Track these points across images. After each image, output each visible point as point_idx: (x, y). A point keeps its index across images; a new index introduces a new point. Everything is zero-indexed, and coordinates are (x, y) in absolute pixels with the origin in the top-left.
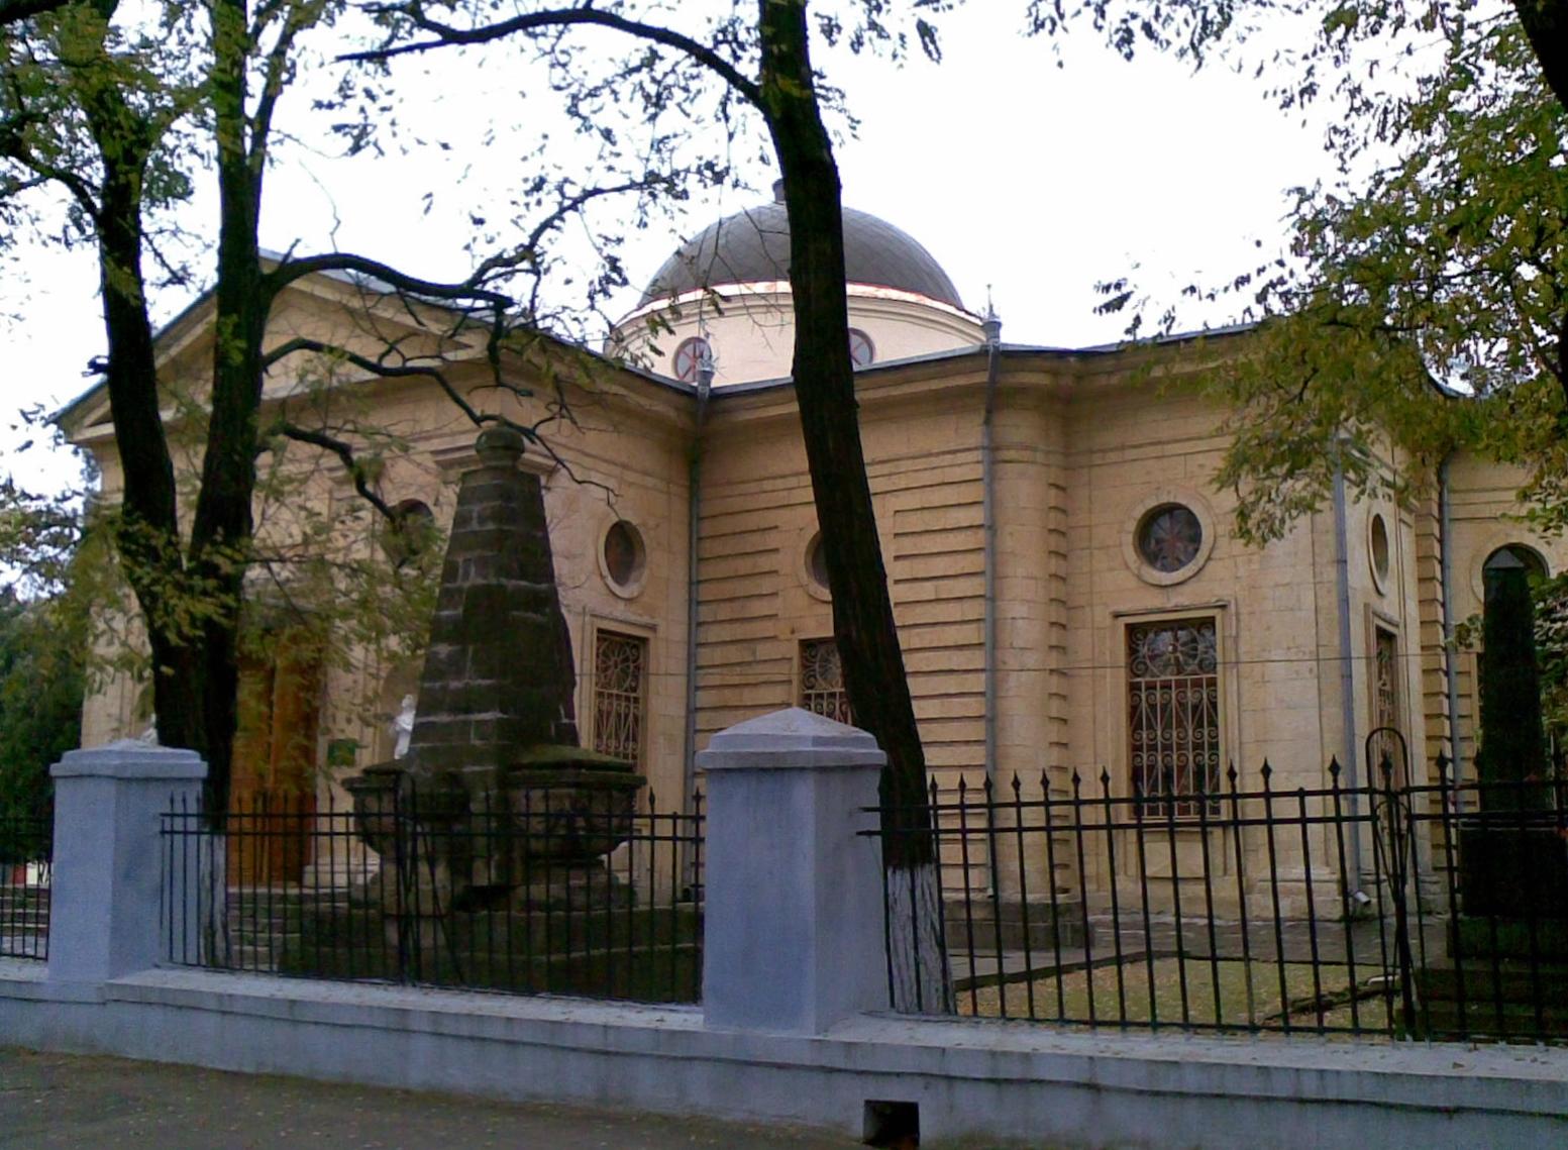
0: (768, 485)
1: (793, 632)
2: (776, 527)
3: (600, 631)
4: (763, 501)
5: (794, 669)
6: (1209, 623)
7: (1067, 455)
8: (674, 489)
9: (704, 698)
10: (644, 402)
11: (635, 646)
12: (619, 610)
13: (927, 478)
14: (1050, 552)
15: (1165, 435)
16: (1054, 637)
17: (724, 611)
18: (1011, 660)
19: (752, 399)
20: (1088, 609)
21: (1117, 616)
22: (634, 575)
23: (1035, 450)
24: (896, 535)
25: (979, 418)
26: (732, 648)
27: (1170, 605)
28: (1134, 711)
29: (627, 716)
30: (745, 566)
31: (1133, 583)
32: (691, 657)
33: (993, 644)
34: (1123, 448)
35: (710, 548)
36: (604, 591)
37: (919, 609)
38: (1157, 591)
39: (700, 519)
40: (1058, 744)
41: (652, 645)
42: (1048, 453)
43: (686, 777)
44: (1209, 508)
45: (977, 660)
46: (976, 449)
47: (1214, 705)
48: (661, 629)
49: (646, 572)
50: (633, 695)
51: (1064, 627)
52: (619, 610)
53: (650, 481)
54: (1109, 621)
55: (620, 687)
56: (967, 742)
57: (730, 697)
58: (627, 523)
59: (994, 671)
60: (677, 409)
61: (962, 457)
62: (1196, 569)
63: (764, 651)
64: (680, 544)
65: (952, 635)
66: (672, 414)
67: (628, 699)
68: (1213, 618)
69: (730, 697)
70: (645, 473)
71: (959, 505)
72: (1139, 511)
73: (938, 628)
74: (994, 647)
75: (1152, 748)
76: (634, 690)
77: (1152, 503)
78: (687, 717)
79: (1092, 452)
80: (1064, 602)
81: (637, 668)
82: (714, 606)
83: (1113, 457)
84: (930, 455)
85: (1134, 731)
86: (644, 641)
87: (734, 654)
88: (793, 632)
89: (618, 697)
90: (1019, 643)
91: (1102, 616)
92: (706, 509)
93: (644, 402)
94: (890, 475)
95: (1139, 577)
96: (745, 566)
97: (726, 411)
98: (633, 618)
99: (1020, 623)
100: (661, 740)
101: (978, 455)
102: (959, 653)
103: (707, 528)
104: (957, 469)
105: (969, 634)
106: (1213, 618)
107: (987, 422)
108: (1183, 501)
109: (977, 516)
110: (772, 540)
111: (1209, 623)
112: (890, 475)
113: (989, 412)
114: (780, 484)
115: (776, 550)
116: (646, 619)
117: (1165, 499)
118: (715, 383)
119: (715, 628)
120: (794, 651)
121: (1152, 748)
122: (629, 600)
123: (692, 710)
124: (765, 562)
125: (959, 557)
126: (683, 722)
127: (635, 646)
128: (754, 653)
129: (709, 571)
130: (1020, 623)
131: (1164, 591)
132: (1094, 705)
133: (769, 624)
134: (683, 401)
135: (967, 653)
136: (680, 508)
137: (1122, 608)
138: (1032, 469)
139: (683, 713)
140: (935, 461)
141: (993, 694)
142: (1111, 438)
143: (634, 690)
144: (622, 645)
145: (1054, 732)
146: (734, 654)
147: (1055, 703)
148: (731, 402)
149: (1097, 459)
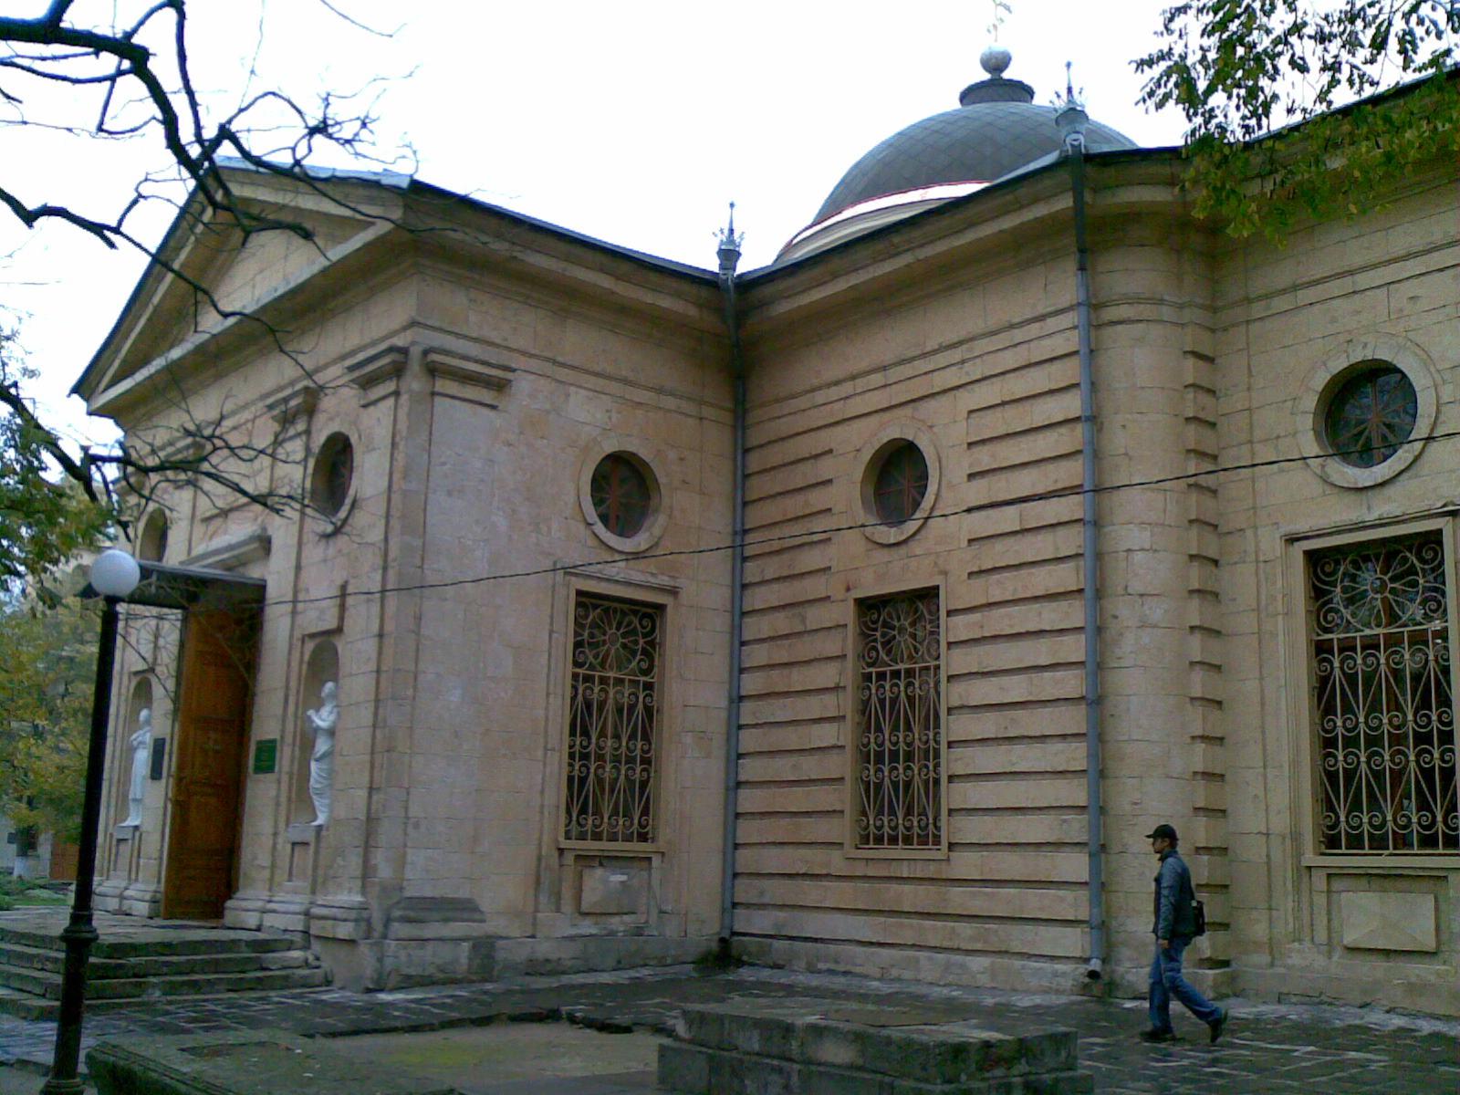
0: (820, 397)
1: (848, 589)
2: (831, 451)
3: (579, 593)
4: (817, 418)
5: (847, 642)
6: (1434, 538)
7: (1215, 310)
8: (707, 412)
9: (751, 684)
10: (649, 298)
11: (645, 615)
12: (619, 570)
13: (1010, 359)
14: (1189, 451)
15: (1358, 261)
16: (1196, 576)
17: (772, 568)
18: (1124, 612)
19: (790, 282)
20: (1249, 533)
21: (1292, 540)
22: (647, 524)
23: (1161, 302)
24: (970, 445)
25: (1071, 265)
26: (781, 615)
27: (1371, 517)
28: (1322, 687)
29: (632, 708)
30: (794, 505)
31: (1318, 487)
32: (736, 629)
33: (1097, 592)
34: (1295, 288)
35: (757, 487)
36: (591, 541)
37: (999, 546)
38: (1353, 497)
39: (746, 451)
40: (1203, 738)
41: (669, 610)
42: (1181, 307)
43: (727, 789)
44: (1428, 361)
45: (1074, 613)
46: (1070, 308)
47: (1446, 671)
48: (683, 596)
49: (661, 519)
50: (642, 679)
51: (1216, 562)
52: (619, 570)
53: (670, 402)
54: (1279, 546)
55: (619, 669)
56: (1064, 737)
57: (778, 680)
58: (634, 454)
59: (1098, 631)
60: (700, 306)
61: (1052, 324)
62: (1410, 458)
63: (816, 616)
64: (720, 482)
65: (1043, 580)
66: (692, 311)
67: (635, 683)
68: (1439, 532)
69: (778, 680)
70: (660, 391)
71: (1052, 392)
72: (1321, 380)
73: (1024, 572)
74: (1099, 594)
75: (1351, 742)
76: (647, 672)
77: (1339, 364)
78: (729, 710)
79: (1248, 300)
80: (1216, 527)
81: (652, 644)
82: (759, 562)
83: (1281, 303)
84: (1012, 327)
85: (1323, 718)
86: (661, 608)
87: (781, 623)
88: (848, 589)
89: (619, 681)
90: (1136, 586)
91: (1270, 543)
92: (755, 438)
93: (649, 298)
94: (963, 362)
95: (1325, 481)
96: (794, 505)
97: (764, 304)
98: (637, 577)
99: (1138, 557)
100: (688, 739)
101: (1070, 319)
102: (1054, 605)
103: (755, 462)
104: (1047, 342)
105: (1065, 577)
106: (1439, 532)
107: (1082, 268)
108: (1384, 355)
109: (1073, 404)
110: (825, 469)
111: (1434, 538)
112: (963, 362)
113: (1082, 251)
114: (834, 393)
115: (830, 481)
116: (664, 580)
117: (1358, 355)
118: (743, 266)
119: (763, 589)
120: (848, 614)
121: (1373, 741)
122: (637, 556)
123: (738, 699)
124: (817, 499)
125: (1050, 467)
126: (724, 715)
127: (645, 615)
128: (803, 620)
129: (756, 516)
130: (1138, 557)
131: (1364, 496)
132: (1261, 679)
133: (823, 578)
134: (705, 293)
135: (1063, 605)
136: (718, 439)
137: (1302, 526)
138: (1155, 331)
139: (724, 703)
140: (1018, 335)
141: (1097, 666)
142: (1282, 275)
143: (647, 672)
144: (624, 613)
145: (1196, 721)
146: (781, 623)
147: (1198, 676)
148: (768, 290)
149: (1257, 310)
